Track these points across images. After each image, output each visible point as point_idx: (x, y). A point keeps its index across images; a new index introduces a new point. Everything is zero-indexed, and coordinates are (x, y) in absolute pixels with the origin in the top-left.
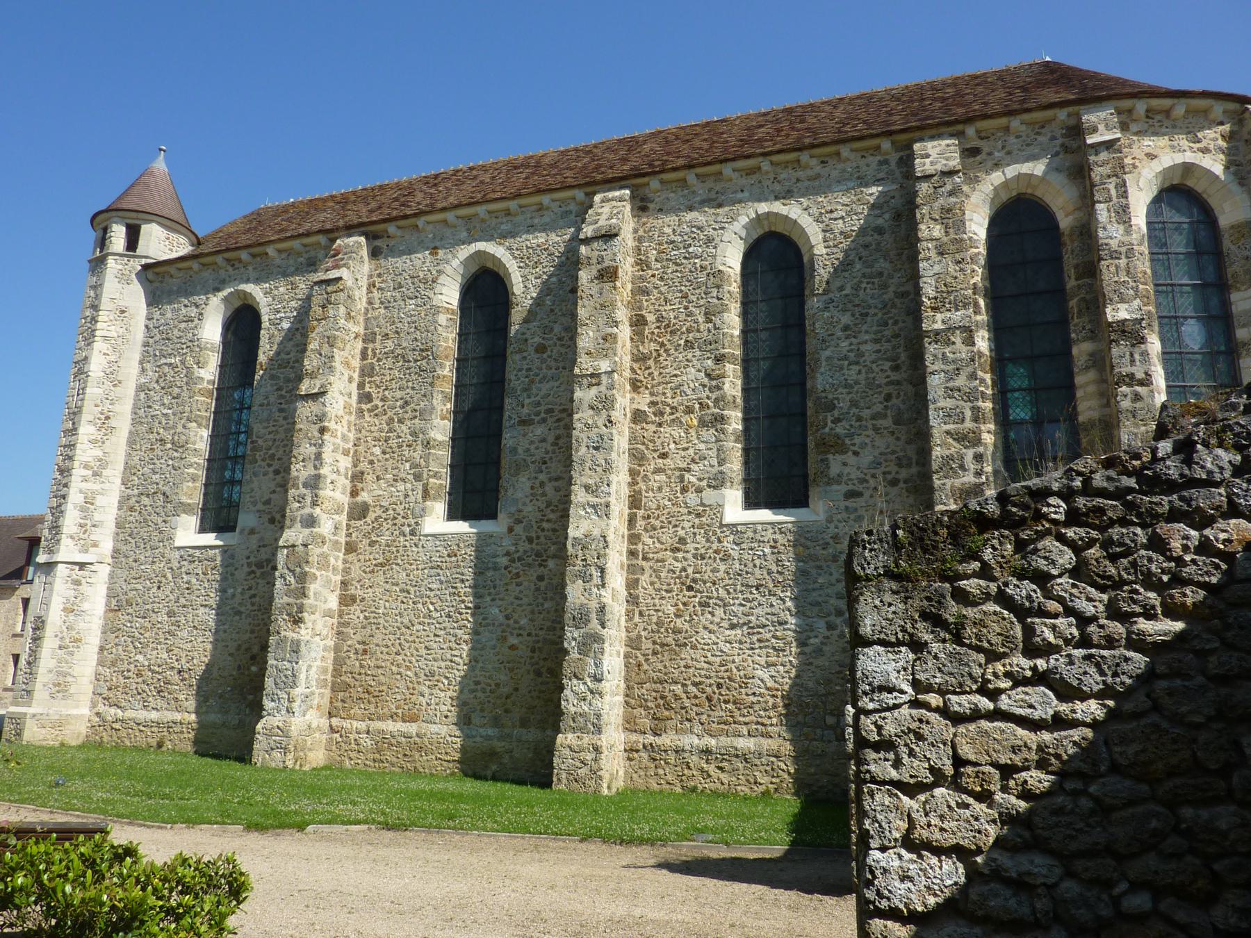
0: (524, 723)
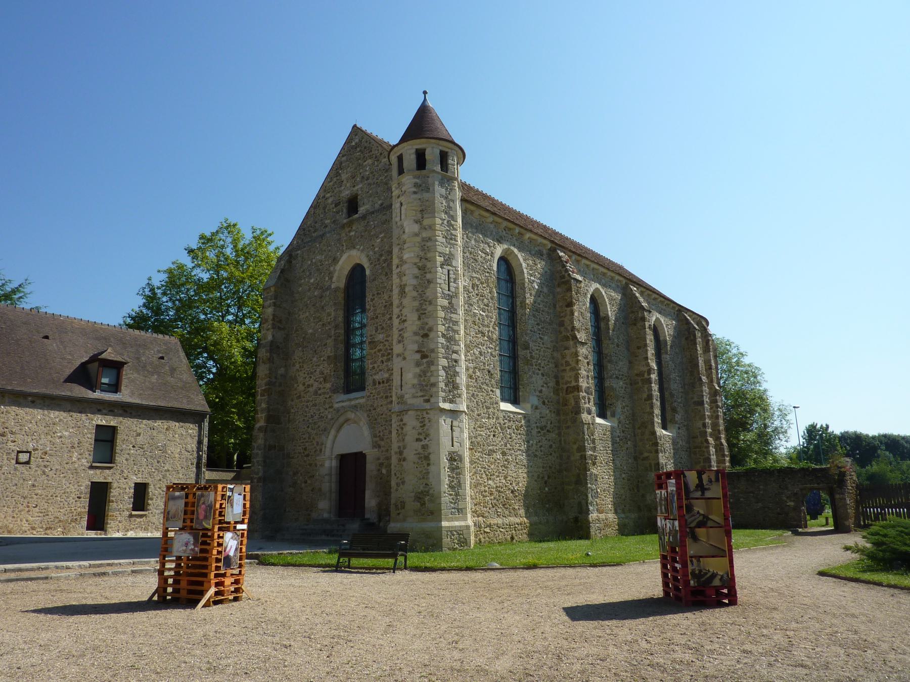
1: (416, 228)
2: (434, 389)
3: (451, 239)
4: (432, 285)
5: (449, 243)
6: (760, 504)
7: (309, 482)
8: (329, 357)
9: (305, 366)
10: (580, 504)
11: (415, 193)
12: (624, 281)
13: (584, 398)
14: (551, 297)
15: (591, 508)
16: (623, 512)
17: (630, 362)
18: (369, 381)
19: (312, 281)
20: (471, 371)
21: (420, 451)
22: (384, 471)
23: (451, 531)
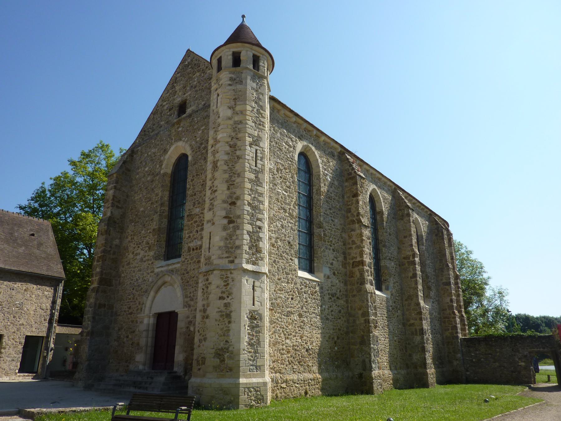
0: (400, 368)
1: (229, 113)
2: (238, 251)
3: (260, 124)
4: (241, 160)
5: (258, 128)
6: (497, 364)
7: (130, 337)
8: (154, 230)
9: (135, 238)
10: (364, 361)
11: (230, 85)
12: (394, 187)
13: (367, 271)
14: (341, 189)
15: (373, 366)
16: (396, 369)
17: (399, 248)
18: (185, 247)
19: (147, 169)
20: (273, 240)
21: (223, 309)
22: (192, 329)
23: (248, 388)
